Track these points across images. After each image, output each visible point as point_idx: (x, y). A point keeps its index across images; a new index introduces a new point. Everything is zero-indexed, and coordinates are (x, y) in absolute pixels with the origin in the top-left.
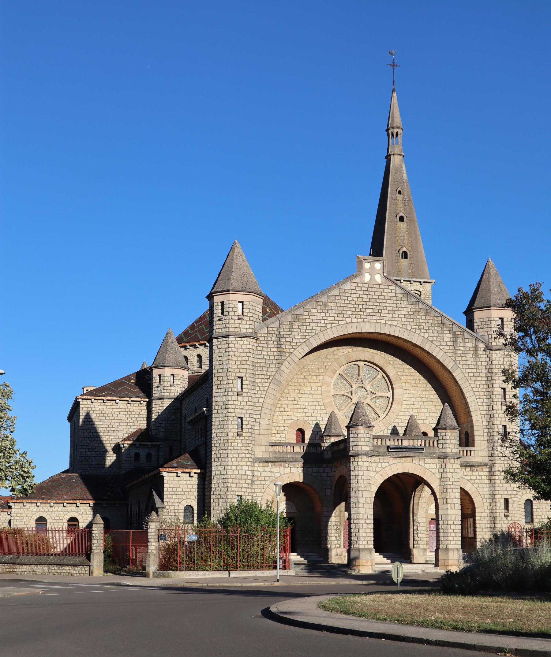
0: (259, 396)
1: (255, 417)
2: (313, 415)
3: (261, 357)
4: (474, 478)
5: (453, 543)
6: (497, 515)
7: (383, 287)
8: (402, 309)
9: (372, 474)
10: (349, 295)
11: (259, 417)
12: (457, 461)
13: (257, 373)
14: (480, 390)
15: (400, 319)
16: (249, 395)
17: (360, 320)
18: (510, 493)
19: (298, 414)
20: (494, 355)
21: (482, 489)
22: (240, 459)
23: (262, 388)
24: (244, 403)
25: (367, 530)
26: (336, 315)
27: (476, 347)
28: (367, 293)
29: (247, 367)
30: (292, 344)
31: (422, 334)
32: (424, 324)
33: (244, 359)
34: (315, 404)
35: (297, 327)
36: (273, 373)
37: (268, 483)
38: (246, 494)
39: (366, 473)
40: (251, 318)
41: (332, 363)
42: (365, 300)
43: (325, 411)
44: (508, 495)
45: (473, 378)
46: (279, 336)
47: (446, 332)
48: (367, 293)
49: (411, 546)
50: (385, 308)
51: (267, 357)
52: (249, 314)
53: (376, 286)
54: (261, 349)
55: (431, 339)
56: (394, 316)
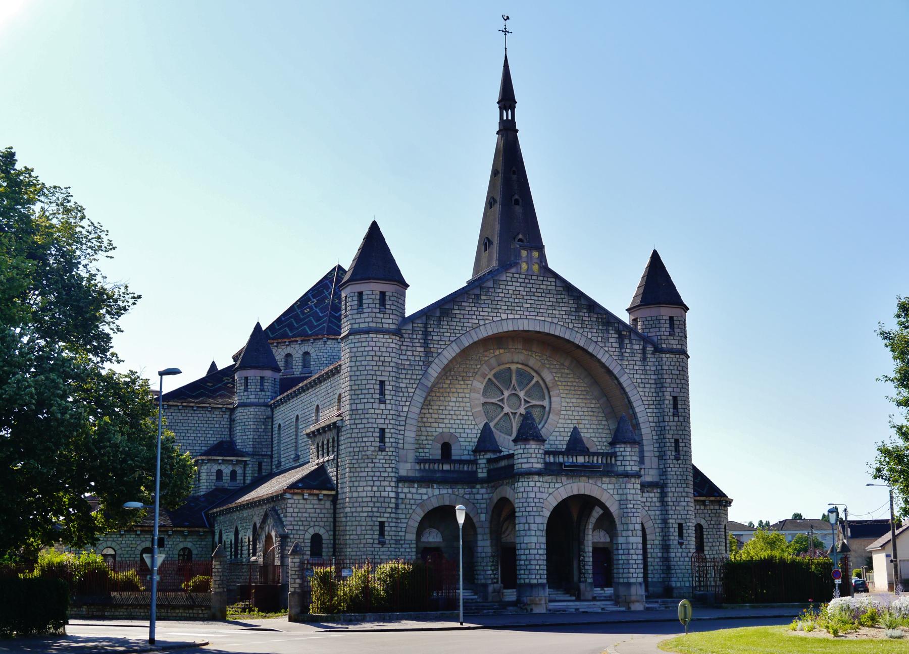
0: (403, 404)
1: (399, 428)
2: (461, 426)
3: (405, 357)
5: (635, 575)
9: (545, 496)
12: (638, 481)
13: (402, 376)
16: (392, 402)
18: (684, 517)
19: (443, 425)
20: (665, 359)
21: (653, 513)
22: (382, 479)
23: (406, 394)
24: (386, 412)
25: (540, 562)
27: (644, 349)
29: (390, 369)
31: (585, 334)
33: (387, 359)
34: (462, 413)
35: (445, 323)
37: (414, 507)
38: (390, 520)
39: (538, 495)
40: (395, 312)
41: (482, 365)
43: (474, 422)
45: (641, 385)
49: (576, 579)
51: (412, 358)
52: (392, 307)
54: (405, 348)
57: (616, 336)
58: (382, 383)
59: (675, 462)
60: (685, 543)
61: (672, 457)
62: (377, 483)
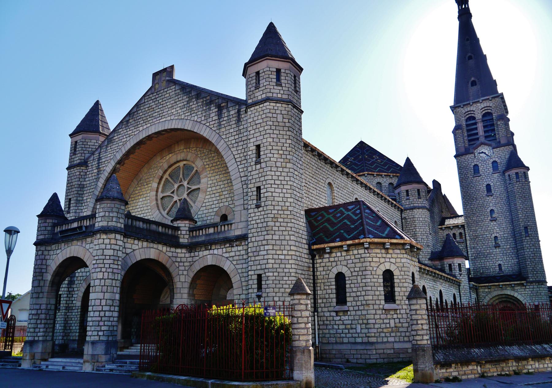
4: (232, 254)
7: (166, 90)
14: (242, 155)
17: (149, 125)
21: (240, 266)
31: (193, 119)
32: (195, 109)
41: (158, 170)
44: (261, 269)
45: (235, 145)
55: (199, 120)
57: (217, 110)
59: (256, 210)
60: (264, 295)
61: (253, 206)
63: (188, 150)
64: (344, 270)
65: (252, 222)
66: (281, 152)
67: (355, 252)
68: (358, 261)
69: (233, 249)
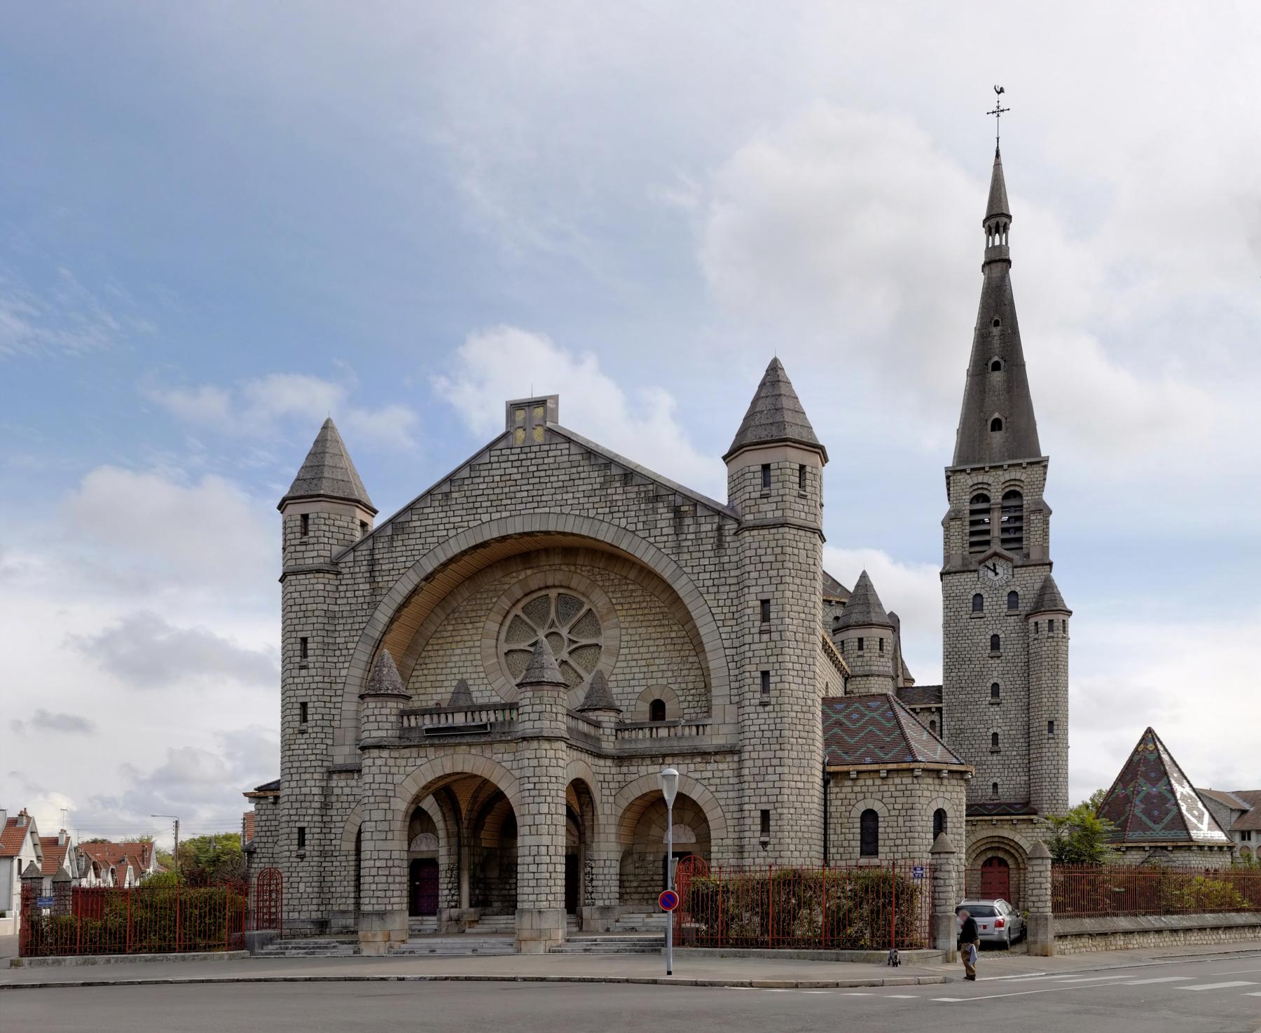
3: (345, 601)
4: (709, 775)
6: (746, 841)
7: (547, 448)
8: (580, 482)
10: (486, 473)
11: (340, 699)
14: (726, 610)
15: (576, 501)
18: (773, 799)
21: (724, 795)
23: (345, 652)
26: (464, 512)
27: (720, 528)
28: (518, 464)
29: (314, 620)
30: (393, 573)
31: (616, 522)
32: (620, 503)
36: (363, 626)
42: (514, 477)
45: (712, 590)
46: (373, 563)
47: (660, 511)
48: (518, 464)
50: (549, 485)
53: (534, 449)
56: (565, 496)
58: (304, 640)
59: (760, 709)
60: (773, 841)
62: (296, 777)
63: (573, 568)
64: (877, 807)
65: (752, 728)
66: (803, 616)
67: (897, 781)
68: (900, 794)
69: (709, 767)
